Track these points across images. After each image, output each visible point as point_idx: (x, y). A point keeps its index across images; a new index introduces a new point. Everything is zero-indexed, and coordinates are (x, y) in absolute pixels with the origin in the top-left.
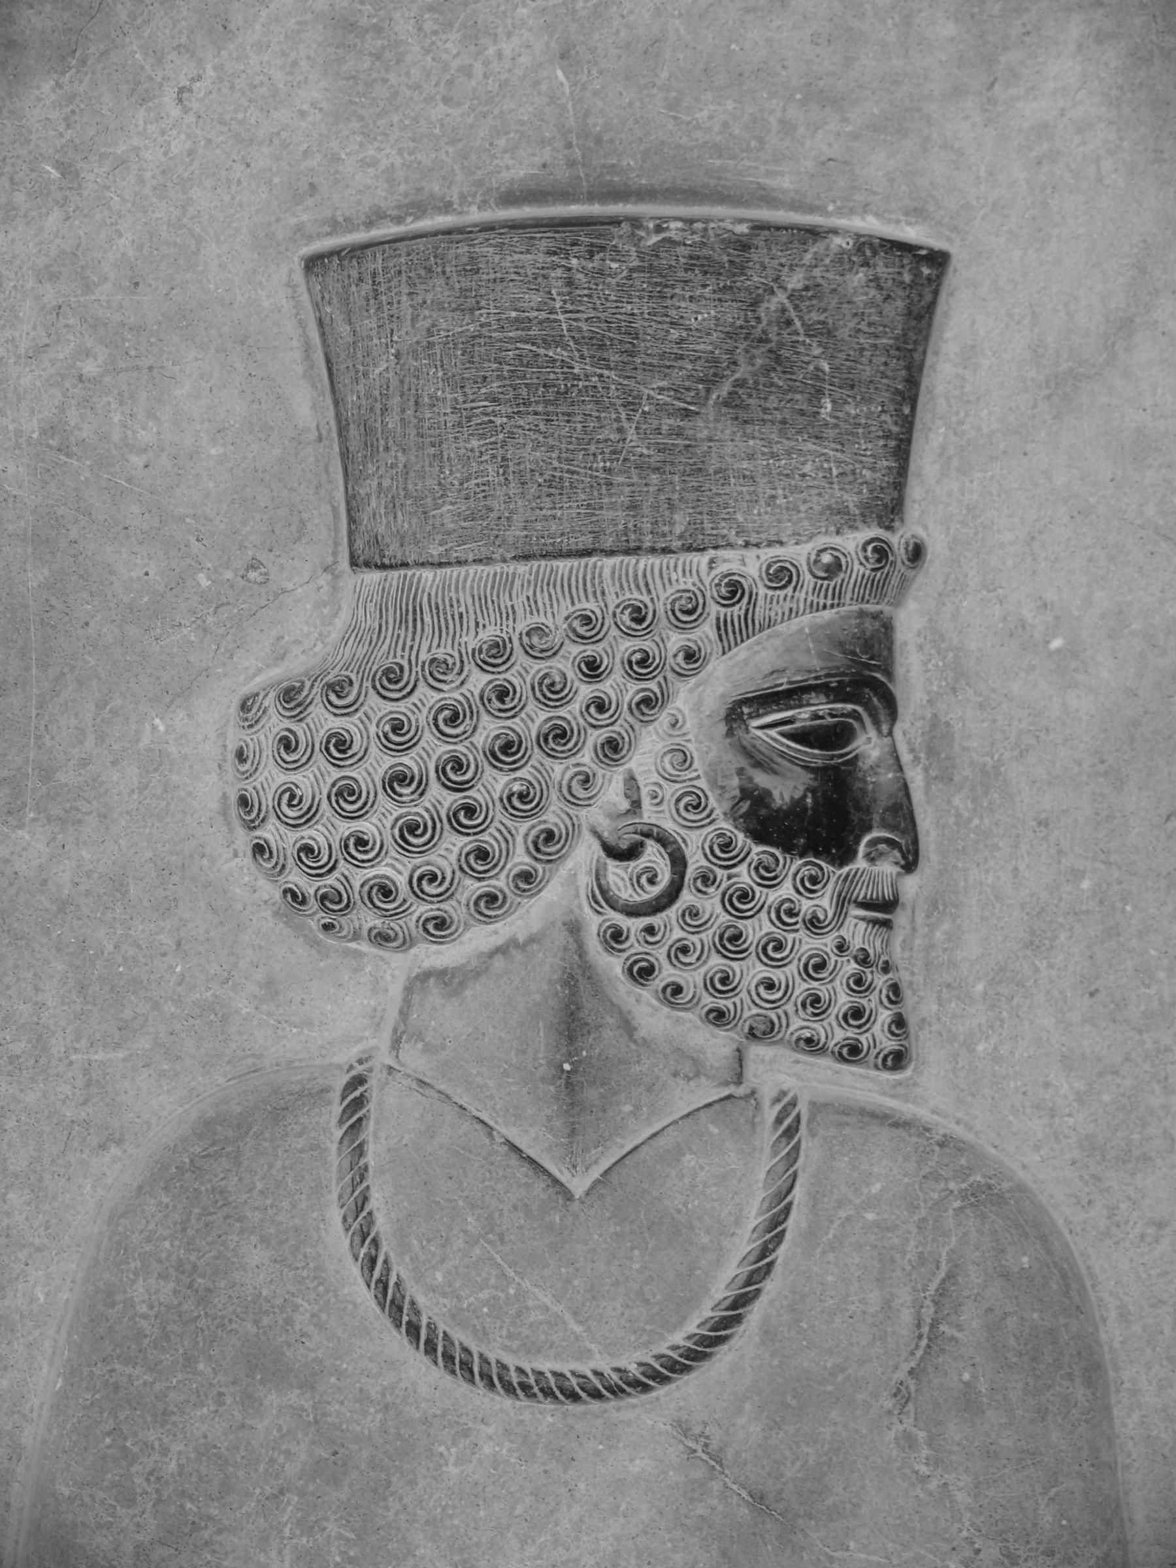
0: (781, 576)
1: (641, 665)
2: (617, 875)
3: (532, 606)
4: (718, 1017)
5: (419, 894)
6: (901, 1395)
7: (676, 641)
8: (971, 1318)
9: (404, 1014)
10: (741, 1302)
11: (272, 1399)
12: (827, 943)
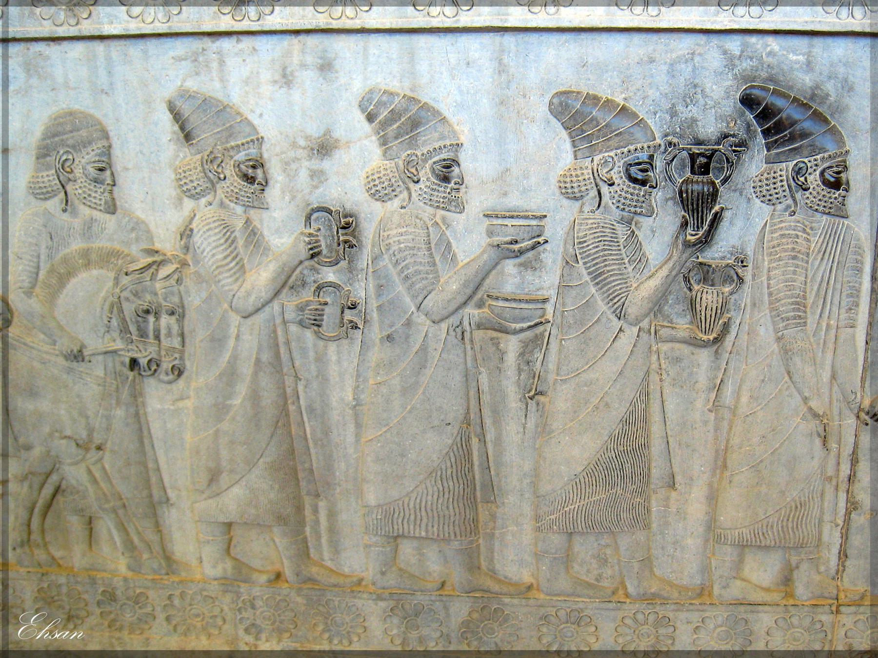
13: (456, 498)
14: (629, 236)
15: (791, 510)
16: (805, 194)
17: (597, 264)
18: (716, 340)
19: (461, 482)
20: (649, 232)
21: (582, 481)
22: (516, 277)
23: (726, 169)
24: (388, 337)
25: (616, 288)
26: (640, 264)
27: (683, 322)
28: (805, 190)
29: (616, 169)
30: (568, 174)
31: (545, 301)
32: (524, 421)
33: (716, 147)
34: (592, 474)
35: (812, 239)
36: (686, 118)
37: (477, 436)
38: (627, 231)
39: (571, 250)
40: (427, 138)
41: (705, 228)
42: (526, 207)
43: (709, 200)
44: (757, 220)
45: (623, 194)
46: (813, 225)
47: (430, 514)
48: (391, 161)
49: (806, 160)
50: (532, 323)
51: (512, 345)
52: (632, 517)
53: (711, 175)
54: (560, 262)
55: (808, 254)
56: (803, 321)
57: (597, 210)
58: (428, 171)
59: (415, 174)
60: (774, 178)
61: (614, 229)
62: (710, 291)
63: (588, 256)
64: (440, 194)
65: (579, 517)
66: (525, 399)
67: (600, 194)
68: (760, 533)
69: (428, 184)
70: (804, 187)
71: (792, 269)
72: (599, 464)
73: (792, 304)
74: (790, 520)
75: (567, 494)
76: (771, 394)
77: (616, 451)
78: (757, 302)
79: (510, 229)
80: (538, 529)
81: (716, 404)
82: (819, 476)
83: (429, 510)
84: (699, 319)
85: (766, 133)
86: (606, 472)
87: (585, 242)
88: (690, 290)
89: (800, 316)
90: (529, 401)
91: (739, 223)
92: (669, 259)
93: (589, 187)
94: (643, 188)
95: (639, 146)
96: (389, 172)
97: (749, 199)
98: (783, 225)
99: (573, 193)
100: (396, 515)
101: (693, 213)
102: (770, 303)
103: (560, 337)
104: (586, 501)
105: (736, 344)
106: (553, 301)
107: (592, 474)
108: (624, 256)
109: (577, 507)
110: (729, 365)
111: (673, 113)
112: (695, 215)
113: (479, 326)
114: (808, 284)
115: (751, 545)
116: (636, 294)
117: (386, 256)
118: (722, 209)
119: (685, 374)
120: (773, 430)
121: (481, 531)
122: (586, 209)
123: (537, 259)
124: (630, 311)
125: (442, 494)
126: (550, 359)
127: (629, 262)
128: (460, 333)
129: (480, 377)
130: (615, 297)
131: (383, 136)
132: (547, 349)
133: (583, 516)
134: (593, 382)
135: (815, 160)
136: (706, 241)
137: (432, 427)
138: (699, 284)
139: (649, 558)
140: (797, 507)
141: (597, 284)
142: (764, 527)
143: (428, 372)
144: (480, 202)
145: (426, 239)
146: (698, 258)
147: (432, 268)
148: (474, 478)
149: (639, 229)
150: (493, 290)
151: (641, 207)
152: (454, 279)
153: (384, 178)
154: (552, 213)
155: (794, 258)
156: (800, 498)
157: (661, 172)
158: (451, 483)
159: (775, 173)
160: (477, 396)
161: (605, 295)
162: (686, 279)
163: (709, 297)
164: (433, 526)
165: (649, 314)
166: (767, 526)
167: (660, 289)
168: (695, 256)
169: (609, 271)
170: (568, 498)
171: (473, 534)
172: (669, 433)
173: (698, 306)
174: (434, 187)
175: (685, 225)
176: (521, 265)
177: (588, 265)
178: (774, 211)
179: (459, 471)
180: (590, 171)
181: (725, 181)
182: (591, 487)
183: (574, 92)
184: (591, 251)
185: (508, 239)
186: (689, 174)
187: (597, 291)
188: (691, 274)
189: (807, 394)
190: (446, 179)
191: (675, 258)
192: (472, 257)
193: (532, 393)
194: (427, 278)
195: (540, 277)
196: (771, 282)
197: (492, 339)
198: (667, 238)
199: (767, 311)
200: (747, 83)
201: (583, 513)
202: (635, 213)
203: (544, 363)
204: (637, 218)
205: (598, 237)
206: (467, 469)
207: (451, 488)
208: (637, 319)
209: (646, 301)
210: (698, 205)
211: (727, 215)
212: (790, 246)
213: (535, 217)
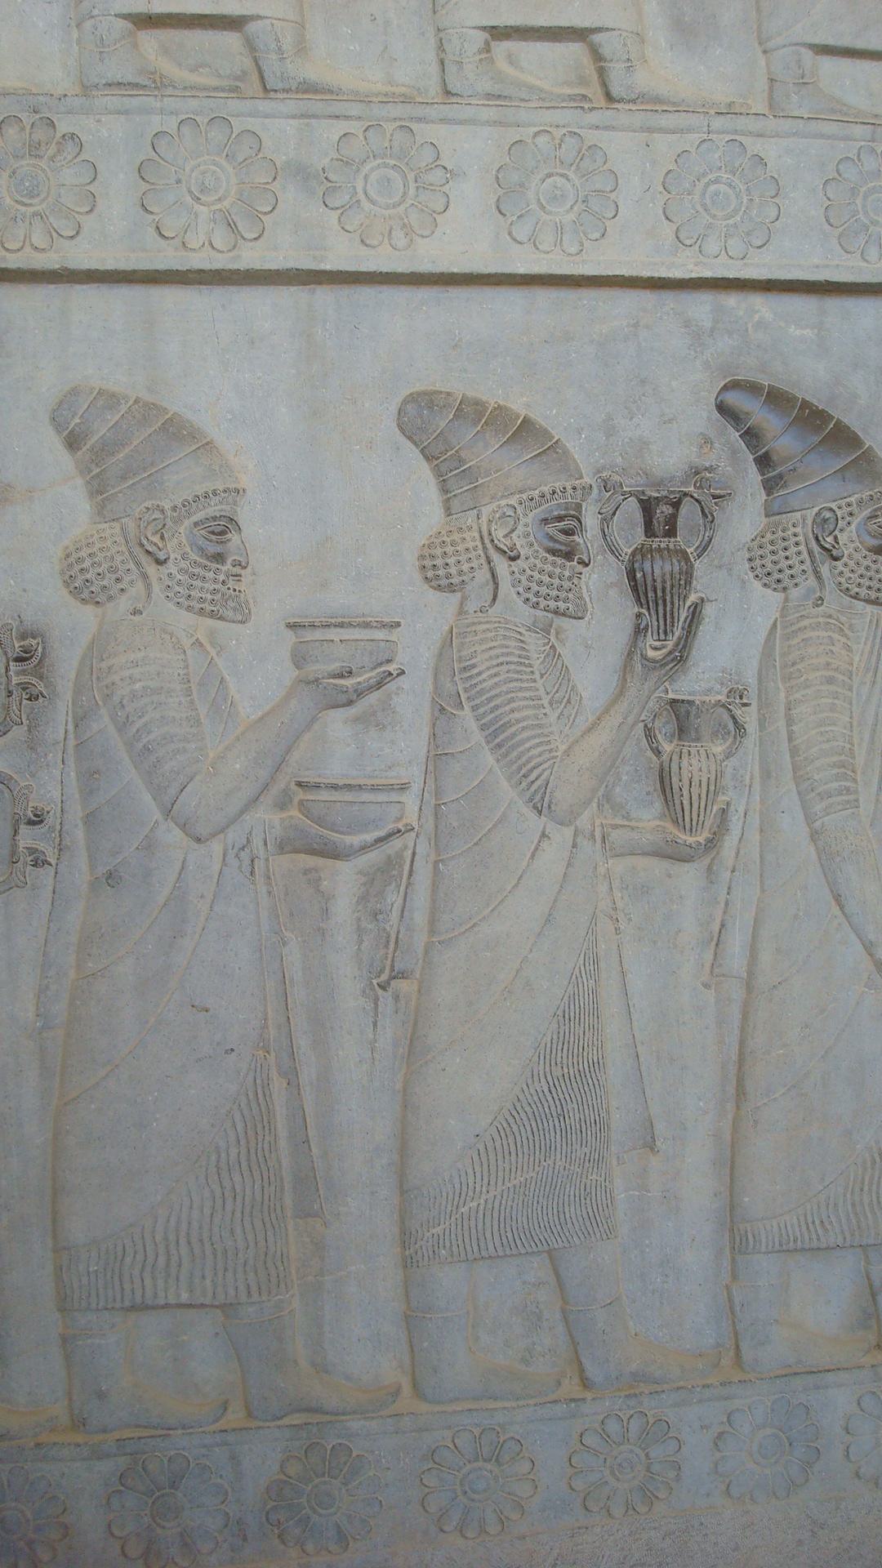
13: (248, 1209)
14: (548, 655)
17: (497, 707)
19: (256, 1174)
21: (490, 1145)
22: (349, 745)
23: (702, 528)
24: (110, 875)
26: (569, 707)
29: (520, 529)
30: (437, 541)
31: (403, 787)
32: (371, 1036)
34: (508, 1129)
41: (677, 634)
43: (682, 582)
44: (759, 619)
47: (197, 1251)
48: (114, 524)
50: (382, 833)
52: (585, 1216)
53: (678, 539)
57: (491, 606)
59: (160, 545)
62: (694, 751)
64: (206, 585)
65: (488, 1224)
66: (373, 989)
67: (494, 576)
69: (183, 564)
81: (716, 971)
84: (678, 807)
87: (474, 666)
90: (380, 992)
96: (109, 543)
99: (448, 576)
100: (128, 1260)
104: (499, 1190)
105: (742, 852)
107: (508, 1129)
109: (482, 1201)
111: (610, 431)
112: (661, 608)
113: (283, 847)
117: (103, 711)
122: (471, 606)
125: (219, 1202)
127: (551, 704)
128: (247, 862)
129: (285, 951)
130: (531, 770)
131: (97, 475)
132: (409, 884)
133: (495, 1223)
136: (680, 658)
141: (499, 746)
145: (182, 672)
146: (667, 692)
150: (307, 773)
153: (100, 557)
158: (237, 1178)
159: (783, 531)
161: (514, 767)
162: (649, 733)
168: (662, 688)
169: (518, 721)
170: (464, 1188)
171: (282, 1286)
173: (675, 780)
174: (196, 571)
176: (357, 720)
177: (481, 710)
178: (786, 600)
179: (253, 1151)
180: (477, 535)
181: (703, 549)
182: (507, 1157)
183: (441, 392)
184: (484, 685)
185: (335, 666)
186: (643, 538)
187: (498, 761)
188: (657, 724)
192: (267, 708)
193: (384, 977)
194: (185, 750)
195: (393, 742)
197: (306, 872)
198: (614, 657)
200: (725, 377)
201: (496, 1215)
202: (556, 612)
203: (406, 913)
206: (266, 1146)
207: (238, 1188)
211: (709, 610)
213: (384, 626)
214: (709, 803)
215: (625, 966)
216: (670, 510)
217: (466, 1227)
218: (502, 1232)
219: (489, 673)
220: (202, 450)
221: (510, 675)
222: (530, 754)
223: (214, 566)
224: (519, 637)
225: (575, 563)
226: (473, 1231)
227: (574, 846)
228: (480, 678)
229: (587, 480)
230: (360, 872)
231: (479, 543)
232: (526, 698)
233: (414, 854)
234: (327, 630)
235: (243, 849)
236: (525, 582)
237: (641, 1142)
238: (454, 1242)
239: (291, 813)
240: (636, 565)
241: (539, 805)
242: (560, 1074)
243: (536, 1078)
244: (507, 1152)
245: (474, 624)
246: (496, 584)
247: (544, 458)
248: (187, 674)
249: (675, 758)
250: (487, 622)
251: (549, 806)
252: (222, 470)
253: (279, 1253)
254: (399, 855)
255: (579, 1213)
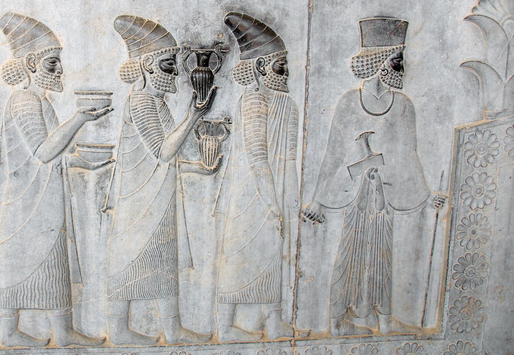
0: (397, 48)
1: (386, 55)
2: (383, 73)
3: (378, 50)
4: (389, 84)
5: (367, 74)
6: (401, 115)
7: (389, 53)
8: (407, 109)
9: (364, 84)
10: (390, 108)
11: (353, 116)
12: (398, 78)
13: (57, 280)
14: (162, 105)
15: (264, 279)
16: (263, 78)
17: (143, 123)
18: (216, 170)
19: (61, 269)
20: (174, 103)
22: (94, 133)
23: (218, 63)
25: (155, 138)
26: (169, 123)
27: (195, 160)
28: (264, 75)
29: (154, 64)
31: (112, 147)
32: (99, 227)
33: (211, 50)
34: (143, 260)
35: (269, 105)
36: (194, 33)
37: (71, 238)
38: (161, 102)
39: (128, 115)
40: (41, 44)
41: (207, 100)
42: (100, 88)
43: (209, 82)
44: (236, 94)
45: (159, 78)
46: (269, 96)
49: (264, 57)
50: (105, 162)
51: (92, 176)
52: (167, 288)
54: (121, 123)
55: (267, 114)
56: (265, 156)
57: (143, 89)
58: (41, 65)
59: (34, 67)
60: (246, 68)
61: (153, 101)
62: (211, 139)
63: (138, 118)
64: (48, 80)
65: (135, 289)
66: (100, 212)
67: (145, 79)
68: (246, 295)
69: (41, 73)
70: (263, 73)
71: (258, 123)
72: (146, 253)
73: (259, 145)
74: (263, 285)
75: (128, 275)
76: (249, 203)
77: (157, 244)
78: (238, 145)
79: (91, 102)
80: (110, 299)
82: (279, 255)
83: (40, 289)
84: (205, 157)
85: (240, 41)
86: (151, 259)
87: (136, 109)
88: (199, 139)
89: (263, 153)
90: (103, 213)
91: (226, 96)
92: (186, 119)
93: (138, 74)
94: (170, 75)
95: (168, 49)
97: (231, 82)
98: (252, 96)
99: (129, 78)
101: (200, 90)
102: (246, 146)
103: (121, 170)
104: (139, 278)
105: (226, 172)
106: (116, 148)
108: (160, 117)
109: (133, 282)
110: (223, 186)
112: (201, 91)
114: (268, 133)
115: (241, 303)
116: (167, 141)
118: (216, 88)
119: (197, 193)
120: (251, 227)
121: (73, 303)
123: (107, 121)
124: (164, 152)
126: (115, 185)
127: (162, 121)
128: (60, 170)
129: (72, 199)
130: (155, 144)
132: (113, 179)
133: (138, 289)
134: (143, 199)
135: (269, 57)
136: (208, 107)
137: (42, 233)
138: (204, 135)
139: (178, 315)
140: (267, 276)
141: (144, 135)
142: (248, 291)
143: (40, 196)
144: (73, 85)
145: (39, 108)
146: (203, 118)
147: (43, 127)
148: (68, 267)
149: (168, 101)
150: (81, 142)
151: (169, 87)
152: (56, 134)
154: (116, 91)
155: (259, 117)
156: (268, 270)
157: (180, 65)
158: (54, 270)
159: (246, 65)
160: (70, 212)
161: (149, 142)
162: (197, 132)
163: (211, 143)
164: (42, 301)
165: (175, 154)
166: (250, 290)
167: (182, 138)
168: (201, 117)
170: (128, 278)
171: (68, 305)
172: (188, 232)
173: (204, 148)
174: (45, 75)
175: (195, 98)
176: (97, 125)
177: (138, 124)
178: (246, 88)
181: (218, 71)
182: (142, 268)
184: (140, 115)
185: (90, 108)
186: (197, 66)
187: (144, 140)
188: (199, 129)
189: (270, 203)
190: (52, 70)
191: (190, 119)
192: (68, 120)
194: (40, 134)
195: (109, 132)
196: (246, 132)
197: (79, 174)
198: (185, 106)
199: (245, 151)
202: (166, 91)
204: (167, 94)
205: (144, 106)
206: (64, 260)
207: (54, 273)
208: (168, 158)
209: (173, 146)
210: (203, 84)
211: (219, 91)
212: (257, 110)
214: (215, 156)
215: (185, 208)
216: (206, 58)
217: (128, 290)
218: (140, 292)
219: (141, 111)
220: (48, 35)
221: (149, 112)
222: (154, 138)
223: (51, 73)
224: (152, 99)
225: (173, 74)
226: (130, 291)
227: (169, 169)
228: (138, 113)
229: (178, 46)
230: (97, 174)
231: (140, 68)
232: (154, 120)
233: (115, 169)
234: (88, 95)
235: (58, 166)
236: (155, 81)
237: (188, 265)
238: (124, 294)
239: (74, 155)
240: (193, 75)
241: (157, 155)
242: (161, 243)
243: (153, 244)
244: (142, 267)
245: (137, 94)
246: (145, 81)
247: (163, 39)
248: (42, 109)
249: (204, 141)
250: (142, 94)
251: (160, 156)
252: (55, 41)
253: (67, 294)
254: (110, 170)
255: (165, 287)
